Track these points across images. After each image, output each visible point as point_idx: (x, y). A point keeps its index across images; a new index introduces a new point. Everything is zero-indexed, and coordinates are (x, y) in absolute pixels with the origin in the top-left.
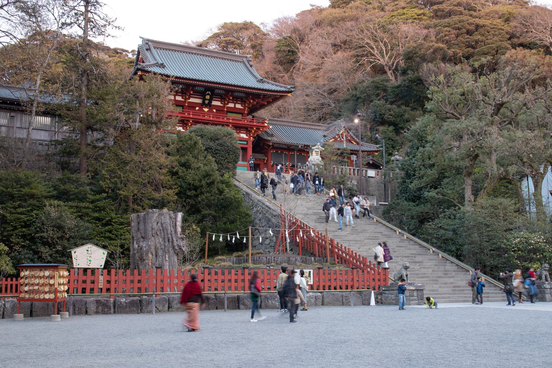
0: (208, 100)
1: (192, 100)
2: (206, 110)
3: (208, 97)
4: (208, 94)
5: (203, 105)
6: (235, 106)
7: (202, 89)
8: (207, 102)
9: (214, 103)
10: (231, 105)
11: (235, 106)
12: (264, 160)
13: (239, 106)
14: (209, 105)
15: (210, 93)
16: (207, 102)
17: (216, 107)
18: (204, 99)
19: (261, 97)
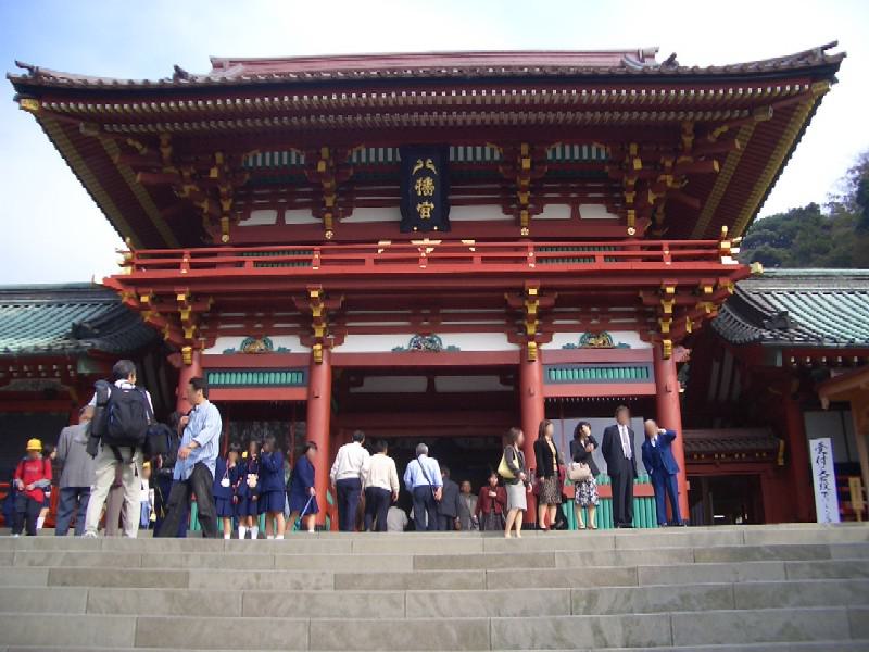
0: (429, 198)
1: (361, 215)
2: (428, 245)
3: (426, 186)
4: (424, 173)
5: (409, 226)
6: (575, 212)
7: (388, 155)
8: (425, 210)
9: (458, 214)
10: (557, 212)
11: (575, 212)
12: (773, 453)
13: (593, 212)
14: (440, 224)
15: (429, 166)
16: (425, 210)
17: (470, 228)
18: (408, 202)
19: (688, 140)
